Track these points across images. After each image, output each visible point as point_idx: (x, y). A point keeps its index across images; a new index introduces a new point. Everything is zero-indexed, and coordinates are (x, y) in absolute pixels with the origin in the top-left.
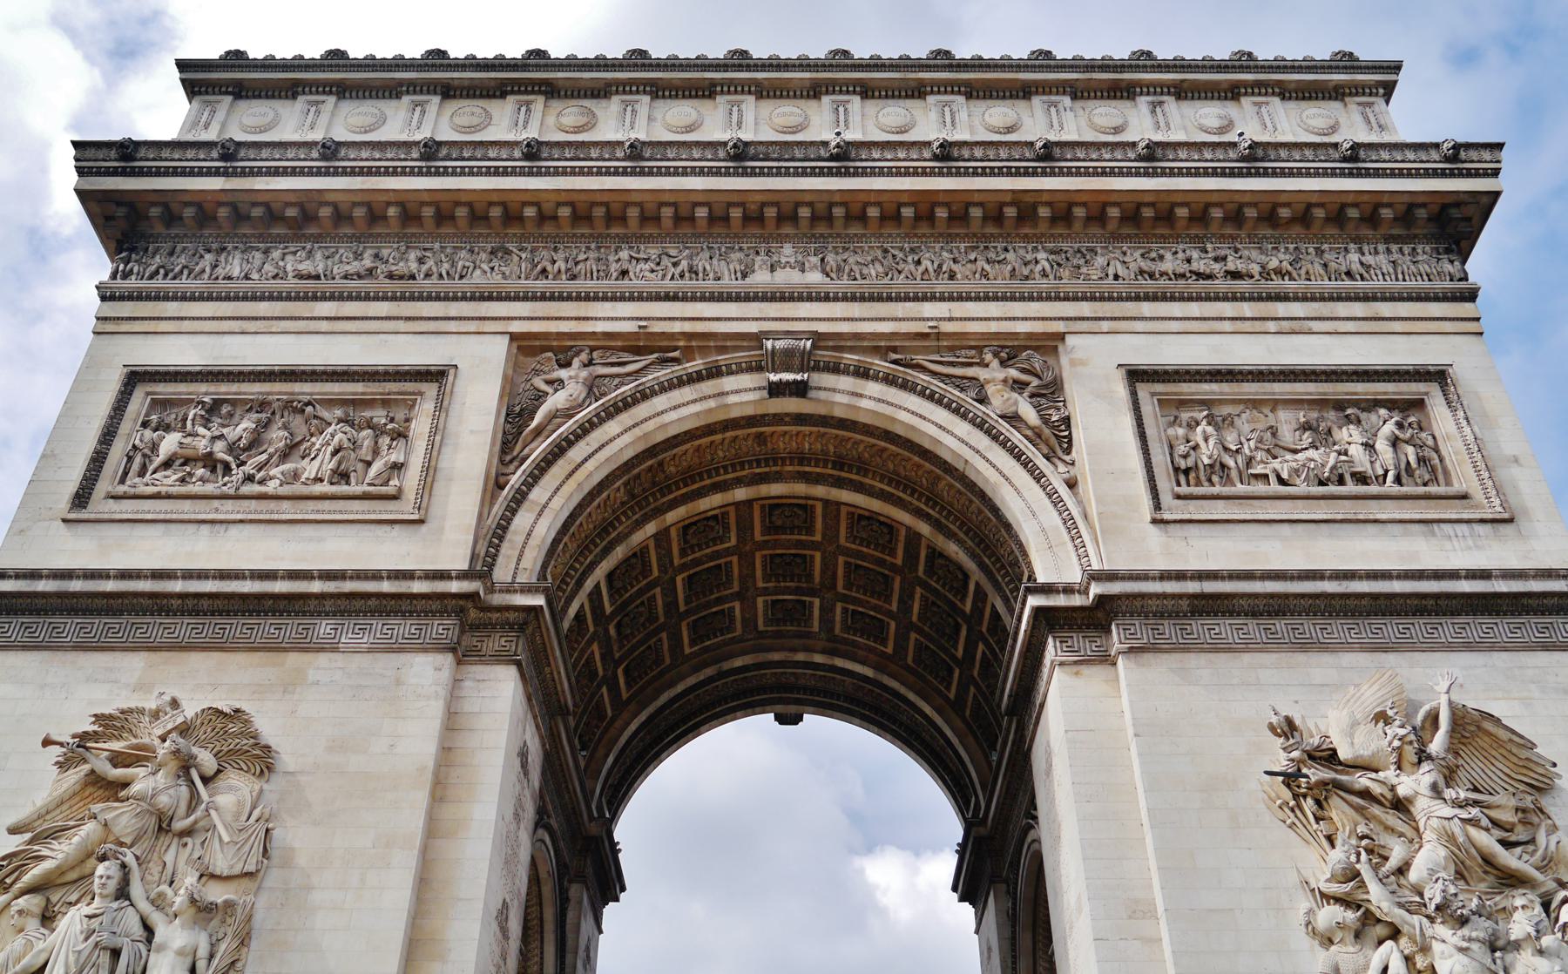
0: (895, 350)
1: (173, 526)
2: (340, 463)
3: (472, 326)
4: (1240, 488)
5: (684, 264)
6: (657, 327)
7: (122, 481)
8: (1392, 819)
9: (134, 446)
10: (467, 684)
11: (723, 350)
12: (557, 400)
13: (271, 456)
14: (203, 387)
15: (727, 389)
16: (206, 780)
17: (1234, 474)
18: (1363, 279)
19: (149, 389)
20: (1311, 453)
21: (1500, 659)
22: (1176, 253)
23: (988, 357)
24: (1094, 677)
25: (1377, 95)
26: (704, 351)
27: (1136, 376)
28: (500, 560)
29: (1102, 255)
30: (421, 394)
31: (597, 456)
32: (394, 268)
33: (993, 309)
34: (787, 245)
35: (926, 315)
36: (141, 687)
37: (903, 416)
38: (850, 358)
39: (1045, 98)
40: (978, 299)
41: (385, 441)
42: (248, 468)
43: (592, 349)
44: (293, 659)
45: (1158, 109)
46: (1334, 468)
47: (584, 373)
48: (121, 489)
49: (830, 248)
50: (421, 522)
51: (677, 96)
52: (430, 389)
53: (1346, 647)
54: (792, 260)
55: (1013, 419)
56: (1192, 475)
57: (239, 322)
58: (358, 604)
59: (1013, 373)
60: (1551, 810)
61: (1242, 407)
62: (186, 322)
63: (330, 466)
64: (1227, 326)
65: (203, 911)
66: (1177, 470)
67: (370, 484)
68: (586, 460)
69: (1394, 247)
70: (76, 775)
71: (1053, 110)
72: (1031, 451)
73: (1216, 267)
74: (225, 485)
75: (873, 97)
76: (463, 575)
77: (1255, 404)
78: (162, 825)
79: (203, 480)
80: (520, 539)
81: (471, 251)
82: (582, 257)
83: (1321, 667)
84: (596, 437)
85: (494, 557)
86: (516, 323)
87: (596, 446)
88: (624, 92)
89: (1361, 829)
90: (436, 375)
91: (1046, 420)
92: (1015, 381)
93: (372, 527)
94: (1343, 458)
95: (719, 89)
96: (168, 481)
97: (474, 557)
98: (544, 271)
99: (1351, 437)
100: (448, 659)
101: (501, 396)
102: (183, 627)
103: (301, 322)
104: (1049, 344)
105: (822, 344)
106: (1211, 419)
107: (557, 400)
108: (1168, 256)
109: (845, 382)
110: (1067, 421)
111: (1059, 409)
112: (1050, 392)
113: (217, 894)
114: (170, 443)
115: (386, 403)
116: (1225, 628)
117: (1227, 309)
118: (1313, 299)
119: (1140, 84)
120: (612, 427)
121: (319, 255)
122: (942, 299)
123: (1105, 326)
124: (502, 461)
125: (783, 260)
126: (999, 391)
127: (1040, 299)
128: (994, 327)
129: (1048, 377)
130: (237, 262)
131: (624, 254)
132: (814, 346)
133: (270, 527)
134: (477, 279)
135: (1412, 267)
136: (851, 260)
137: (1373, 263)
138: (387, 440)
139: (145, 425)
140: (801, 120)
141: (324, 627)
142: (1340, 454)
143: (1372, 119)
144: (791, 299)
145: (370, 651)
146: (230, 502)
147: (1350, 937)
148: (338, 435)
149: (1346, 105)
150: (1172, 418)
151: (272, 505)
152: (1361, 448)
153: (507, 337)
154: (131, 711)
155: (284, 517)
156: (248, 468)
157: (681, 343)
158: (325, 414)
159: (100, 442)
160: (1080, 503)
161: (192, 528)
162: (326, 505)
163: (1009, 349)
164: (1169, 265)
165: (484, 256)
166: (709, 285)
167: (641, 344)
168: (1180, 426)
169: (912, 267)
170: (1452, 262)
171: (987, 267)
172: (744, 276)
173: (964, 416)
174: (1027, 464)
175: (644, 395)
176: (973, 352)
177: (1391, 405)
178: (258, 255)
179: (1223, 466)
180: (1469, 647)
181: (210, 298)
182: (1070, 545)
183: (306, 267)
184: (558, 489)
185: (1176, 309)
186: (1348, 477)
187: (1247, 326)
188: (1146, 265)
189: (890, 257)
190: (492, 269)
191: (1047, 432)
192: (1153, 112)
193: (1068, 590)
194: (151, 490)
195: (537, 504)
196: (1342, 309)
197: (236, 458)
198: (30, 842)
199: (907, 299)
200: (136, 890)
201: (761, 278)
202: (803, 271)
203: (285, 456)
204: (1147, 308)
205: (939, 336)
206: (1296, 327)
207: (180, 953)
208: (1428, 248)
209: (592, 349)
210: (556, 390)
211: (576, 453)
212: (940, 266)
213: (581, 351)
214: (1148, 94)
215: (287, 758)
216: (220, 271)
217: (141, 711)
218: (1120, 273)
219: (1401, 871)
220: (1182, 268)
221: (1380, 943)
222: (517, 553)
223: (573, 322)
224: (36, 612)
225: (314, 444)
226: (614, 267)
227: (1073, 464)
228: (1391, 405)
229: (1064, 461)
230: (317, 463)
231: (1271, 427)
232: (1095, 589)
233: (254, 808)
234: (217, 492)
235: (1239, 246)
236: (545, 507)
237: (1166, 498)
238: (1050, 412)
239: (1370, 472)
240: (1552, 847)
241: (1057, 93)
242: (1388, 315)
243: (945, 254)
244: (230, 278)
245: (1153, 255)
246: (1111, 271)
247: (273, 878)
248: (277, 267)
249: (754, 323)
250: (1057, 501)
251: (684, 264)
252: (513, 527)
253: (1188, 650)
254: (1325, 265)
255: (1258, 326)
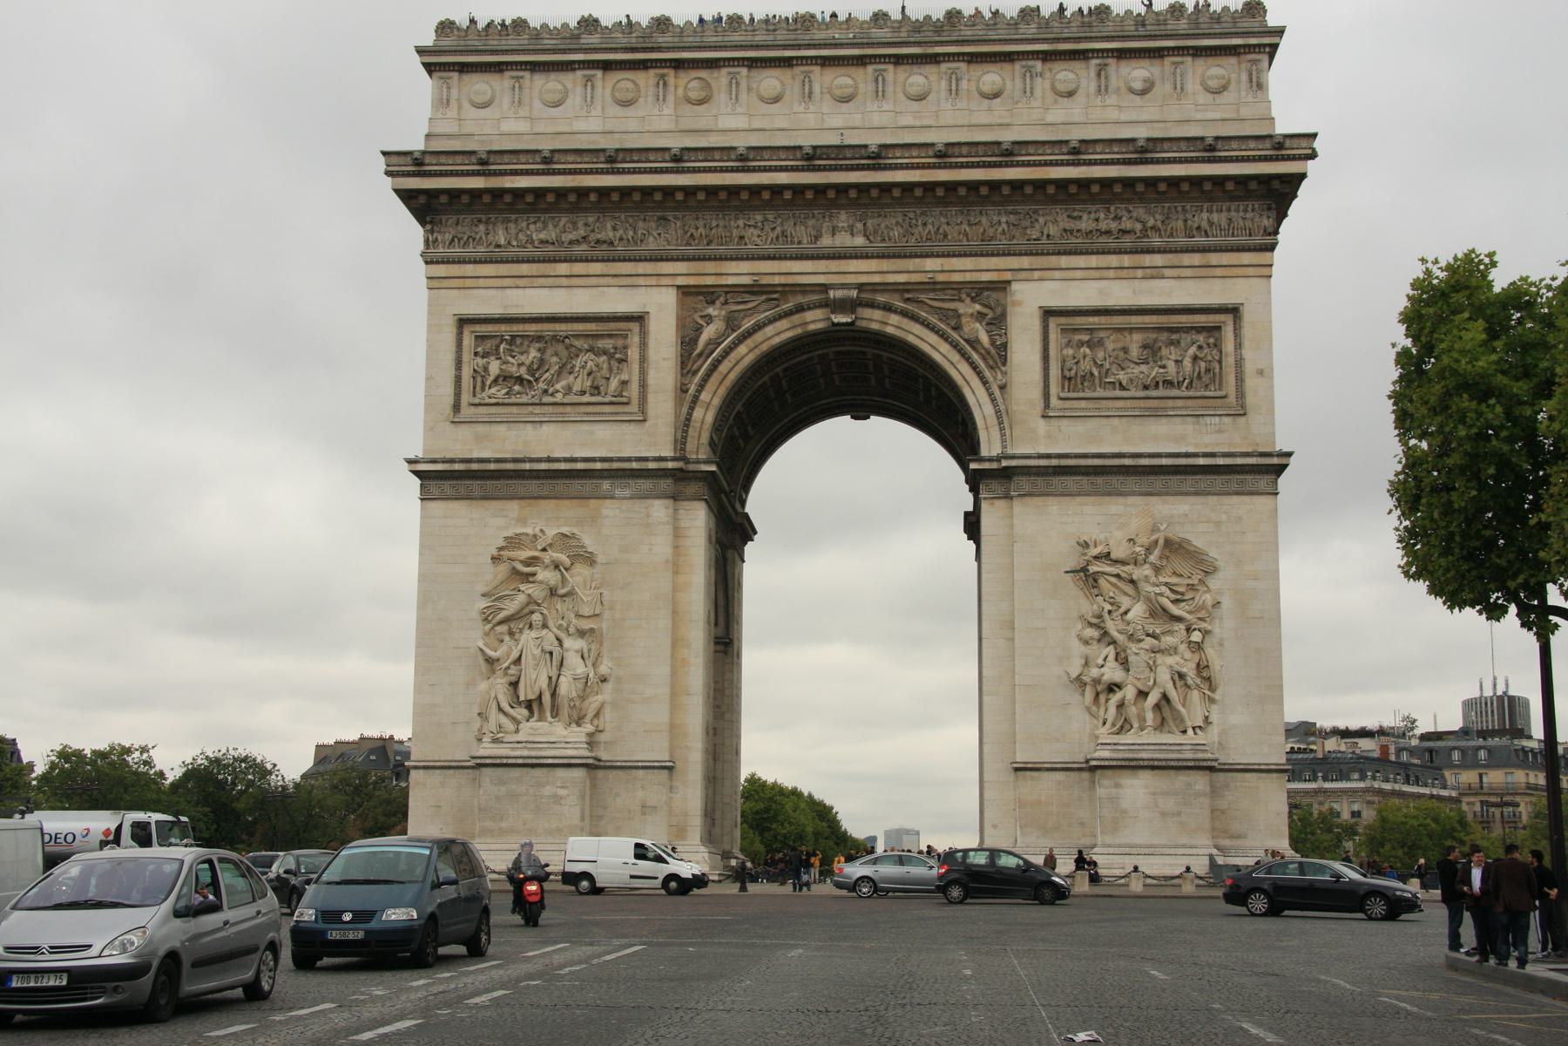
0: (908, 291)
1: (512, 425)
2: (593, 382)
3: (653, 281)
4: (1100, 393)
5: (779, 229)
6: (765, 280)
7: (474, 396)
8: (1129, 589)
9: (474, 370)
10: (681, 511)
11: (804, 293)
12: (709, 332)
13: (553, 375)
14: (503, 327)
15: (808, 320)
16: (566, 569)
17: (1097, 381)
18: (1207, 236)
19: (472, 329)
20: (1144, 368)
21: (1212, 499)
22: (1090, 213)
23: (964, 296)
24: (1001, 504)
25: (1264, 52)
26: (794, 293)
27: (1048, 313)
28: (689, 439)
29: (1043, 215)
30: (630, 330)
31: (735, 369)
32: (599, 236)
33: (967, 263)
34: (843, 212)
35: (928, 269)
36: (522, 520)
37: (911, 339)
38: (881, 298)
39: (1024, 63)
40: (960, 255)
41: (615, 364)
42: (542, 385)
43: (727, 293)
44: (592, 502)
45: (1103, 73)
46: (1154, 378)
47: (723, 313)
48: (477, 401)
49: (870, 214)
50: (645, 420)
51: (766, 67)
52: (635, 327)
53: (1133, 494)
54: (845, 225)
55: (974, 343)
56: (1073, 382)
57: (513, 279)
58: (620, 473)
59: (978, 307)
60: (1211, 586)
61: (1111, 331)
62: (481, 280)
63: (589, 384)
64: (1111, 273)
65: (581, 633)
66: (1064, 377)
67: (613, 396)
68: (729, 372)
69: (1234, 206)
70: (503, 569)
71: (1028, 75)
72: (982, 365)
73: (1114, 226)
74: (533, 397)
75: (903, 64)
76: (674, 459)
77: (1120, 330)
78: (553, 592)
79: (518, 393)
80: (698, 425)
81: (645, 220)
82: (714, 223)
83: (1116, 506)
84: (734, 356)
85: (685, 438)
86: (680, 278)
87: (734, 362)
88: (729, 66)
89: (1111, 594)
90: (639, 319)
91: (993, 343)
92: (979, 313)
93: (619, 424)
94: (1162, 370)
95: (795, 62)
96: (499, 392)
97: (675, 449)
98: (692, 235)
99: (1170, 355)
100: (669, 502)
101: (677, 331)
102: (533, 486)
103: (550, 279)
104: (1002, 286)
105: (864, 288)
106: (1089, 344)
107: (709, 332)
108: (1085, 217)
109: (877, 314)
110: (1005, 346)
111: (1000, 335)
112: (997, 321)
113: (586, 625)
114: (494, 367)
115: (610, 336)
116: (1070, 482)
117: (1113, 260)
118: (1170, 252)
119: (1093, 51)
120: (742, 349)
121: (550, 226)
122: (938, 256)
123: (1037, 274)
124: (682, 375)
125: (841, 225)
126: (968, 322)
127: (998, 255)
128: (968, 277)
129: (999, 311)
130: (500, 232)
131: (741, 223)
132: (858, 293)
133: (564, 424)
134: (652, 244)
135: (1241, 223)
136: (883, 225)
137: (1216, 220)
138: (617, 364)
139: (476, 354)
140: (850, 90)
141: (606, 485)
142: (1160, 367)
143: (1254, 80)
144: (845, 257)
145: (631, 498)
146: (538, 407)
147: (1095, 643)
148: (589, 360)
149: (1239, 63)
150: (1067, 340)
151: (561, 409)
152: (1173, 363)
153: (675, 288)
154: (521, 534)
155: (571, 419)
156: (542, 385)
157: (780, 289)
158: (577, 343)
159: (456, 370)
160: (1004, 399)
161: (522, 425)
162: (591, 409)
163: (977, 290)
164: (1085, 224)
165: (653, 225)
166: (793, 248)
167: (755, 290)
168: (1072, 347)
169: (920, 228)
170: (1269, 217)
171: (967, 229)
172: (817, 238)
173: (946, 340)
174: (979, 374)
175: (759, 327)
176: (955, 292)
177: (1200, 330)
178: (512, 225)
179: (1092, 374)
180: (1196, 494)
181: (491, 262)
182: (997, 428)
183: (542, 236)
184: (715, 392)
185: (1081, 261)
186: (1161, 384)
187: (1124, 273)
188: (1070, 225)
189: (908, 220)
190: (659, 234)
191: (993, 351)
192: (1099, 75)
193: (990, 460)
194: (493, 401)
195: (704, 402)
196: (1187, 259)
197: (533, 376)
198: (493, 601)
199: (916, 256)
200: (551, 624)
201: (826, 241)
202: (852, 234)
203: (559, 373)
204: (1064, 261)
205: (935, 283)
206: (1155, 274)
207: (577, 652)
208: (1256, 206)
209: (727, 293)
210: (708, 324)
211: (723, 368)
212: (938, 229)
213: (720, 296)
214: (1098, 57)
215: (600, 559)
216: (491, 237)
217: (527, 535)
218: (1051, 233)
219: (1126, 613)
220: (1092, 226)
221: (1109, 644)
222: (697, 435)
223: (713, 277)
224: (457, 478)
225: (574, 366)
226: (735, 233)
227: (1006, 373)
228: (1200, 330)
229: (1001, 371)
230: (579, 380)
231: (1124, 348)
232: (1004, 463)
233: (592, 581)
234: (530, 402)
235: (1131, 209)
236: (709, 404)
237: (1054, 401)
238: (997, 337)
239: (1176, 381)
240: (1201, 602)
241: (1033, 59)
242: (1214, 264)
243: (943, 220)
244: (499, 246)
245: (1076, 214)
246: (1045, 233)
247: (607, 615)
248: (527, 236)
249: (823, 276)
250: (993, 400)
251: (779, 229)
252: (693, 418)
253: (1047, 495)
254: (1185, 221)
255: (1131, 273)
